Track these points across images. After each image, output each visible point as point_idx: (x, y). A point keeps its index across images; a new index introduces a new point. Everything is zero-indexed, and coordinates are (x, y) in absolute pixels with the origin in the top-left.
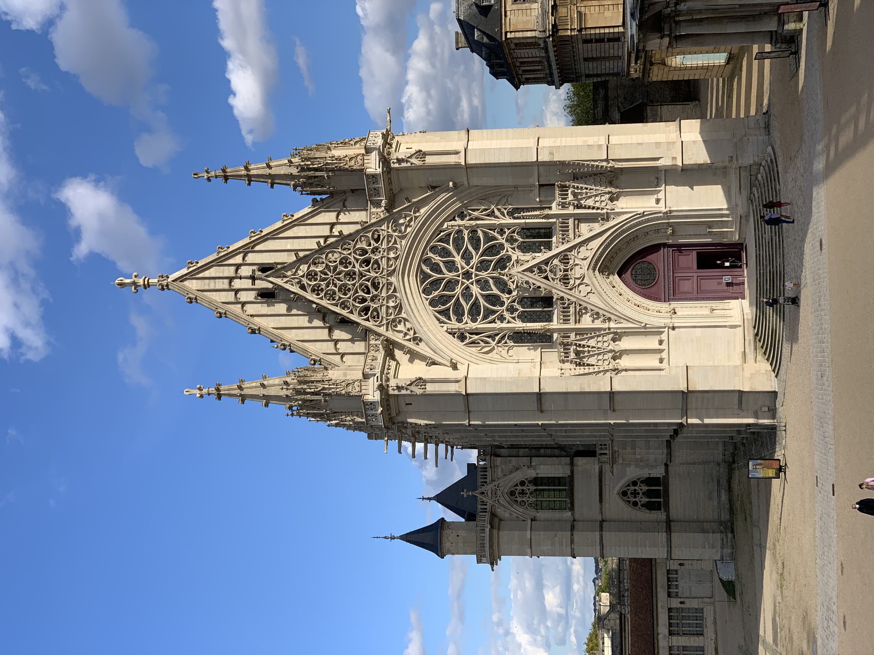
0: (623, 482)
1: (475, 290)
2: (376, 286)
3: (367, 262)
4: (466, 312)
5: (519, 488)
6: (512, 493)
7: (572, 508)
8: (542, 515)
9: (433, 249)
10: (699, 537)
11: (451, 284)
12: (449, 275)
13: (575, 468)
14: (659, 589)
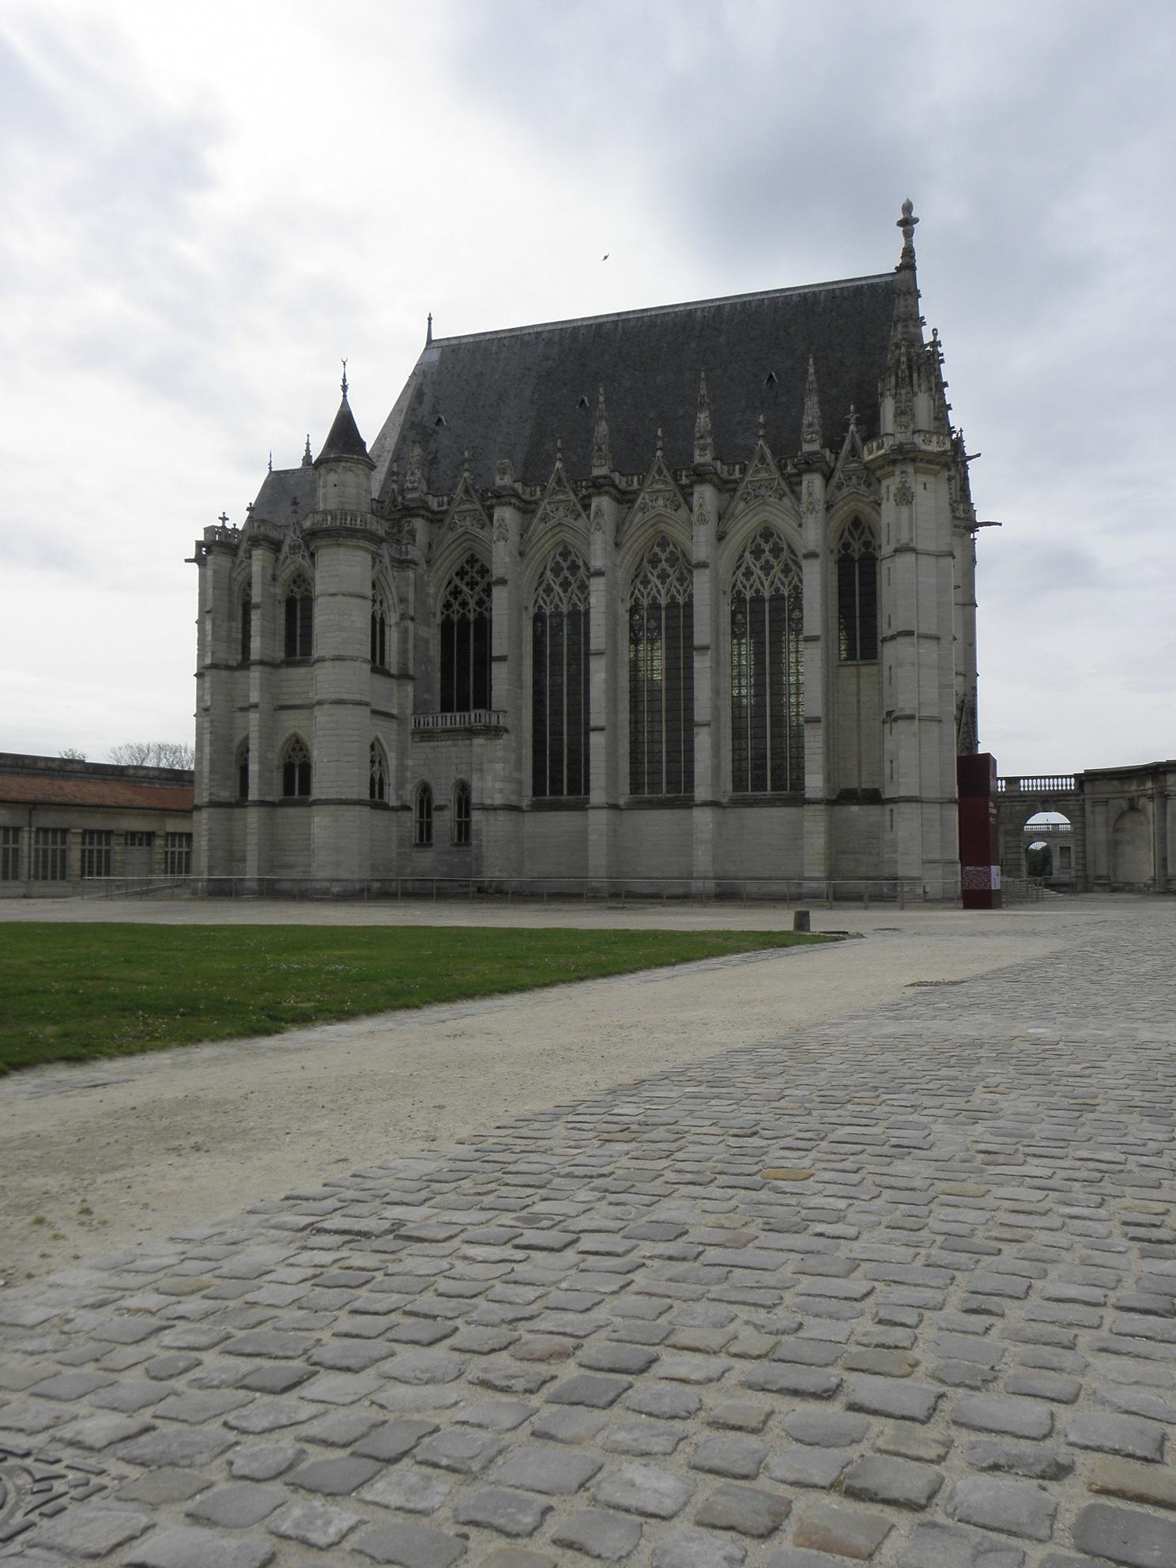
0: (385, 746)
13: (394, 681)
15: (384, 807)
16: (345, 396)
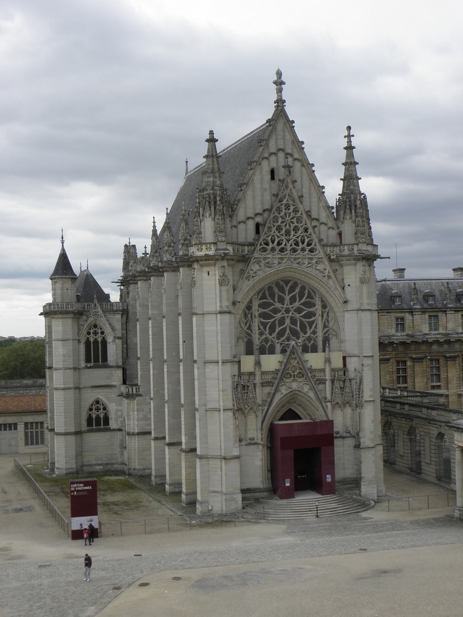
1: (279, 316)
2: (282, 250)
3: (297, 244)
4: (265, 310)
5: (99, 331)
6: (95, 326)
7: (87, 367)
8: (82, 347)
9: (303, 288)
10: (73, 453)
11: (281, 300)
12: (287, 298)
13: (114, 369)
14: (3, 418)
15: (109, 430)
16: (63, 246)
